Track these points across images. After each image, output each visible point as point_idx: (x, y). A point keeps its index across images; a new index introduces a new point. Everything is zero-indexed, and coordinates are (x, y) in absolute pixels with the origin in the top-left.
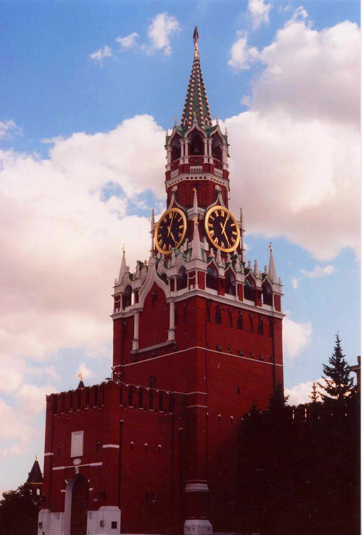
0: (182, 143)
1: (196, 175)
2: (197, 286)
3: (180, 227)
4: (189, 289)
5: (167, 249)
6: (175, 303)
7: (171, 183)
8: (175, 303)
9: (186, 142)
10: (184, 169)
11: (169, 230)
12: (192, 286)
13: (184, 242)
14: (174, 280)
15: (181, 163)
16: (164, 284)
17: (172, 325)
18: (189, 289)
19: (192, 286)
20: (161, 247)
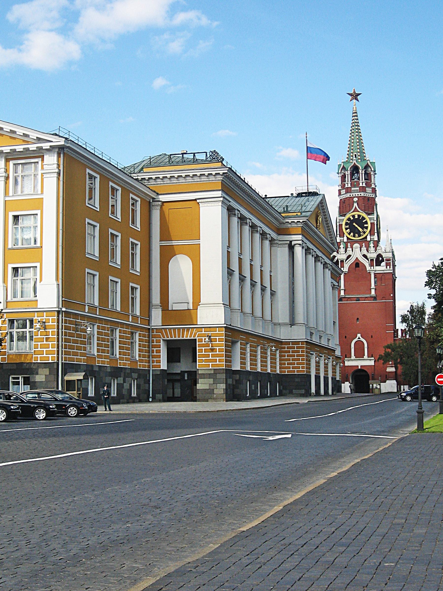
0: (361, 172)
1: (369, 193)
2: (391, 267)
3: (365, 225)
4: (387, 268)
5: (354, 236)
6: (375, 273)
7: (351, 195)
8: (375, 273)
9: (363, 172)
10: (363, 189)
11: (356, 226)
12: (388, 267)
13: (367, 235)
14: (373, 260)
15: (361, 185)
16: (367, 261)
17: (373, 286)
18: (387, 268)
19: (388, 267)
20: (349, 234)
